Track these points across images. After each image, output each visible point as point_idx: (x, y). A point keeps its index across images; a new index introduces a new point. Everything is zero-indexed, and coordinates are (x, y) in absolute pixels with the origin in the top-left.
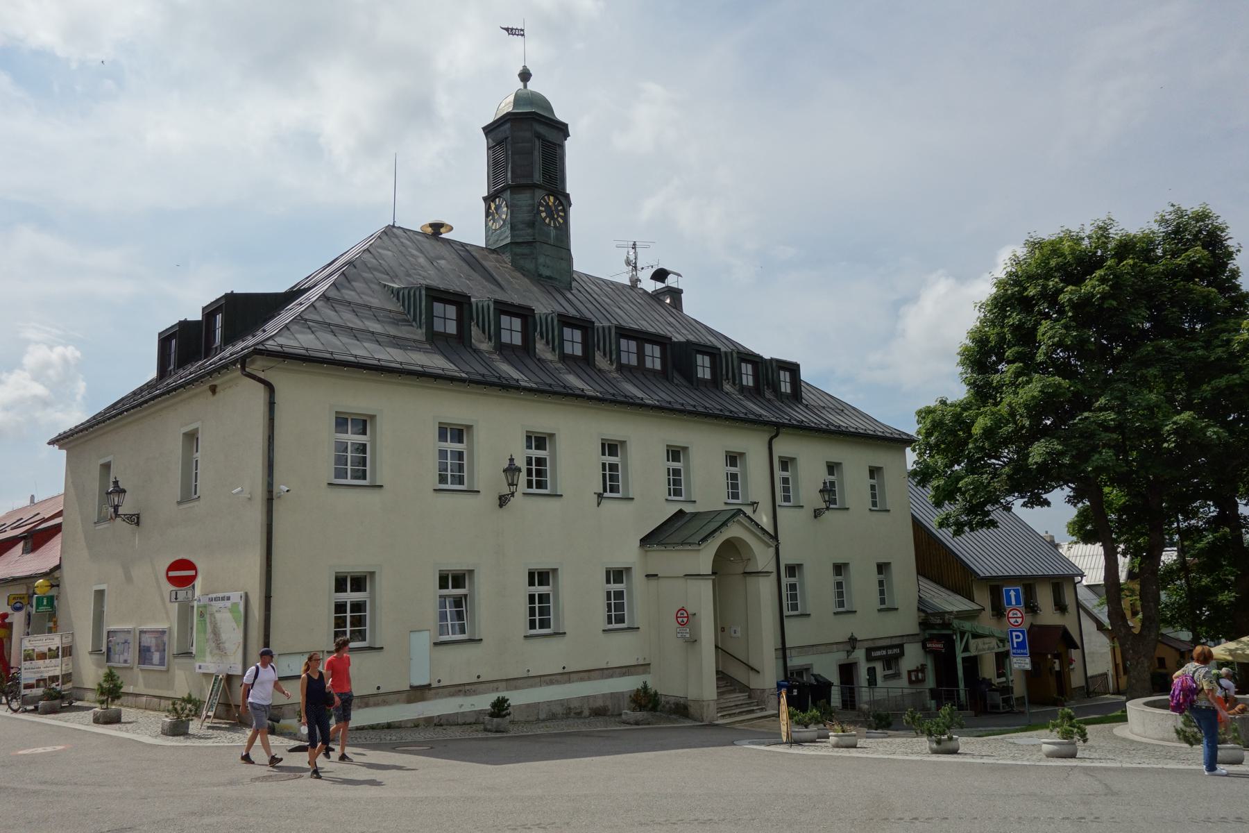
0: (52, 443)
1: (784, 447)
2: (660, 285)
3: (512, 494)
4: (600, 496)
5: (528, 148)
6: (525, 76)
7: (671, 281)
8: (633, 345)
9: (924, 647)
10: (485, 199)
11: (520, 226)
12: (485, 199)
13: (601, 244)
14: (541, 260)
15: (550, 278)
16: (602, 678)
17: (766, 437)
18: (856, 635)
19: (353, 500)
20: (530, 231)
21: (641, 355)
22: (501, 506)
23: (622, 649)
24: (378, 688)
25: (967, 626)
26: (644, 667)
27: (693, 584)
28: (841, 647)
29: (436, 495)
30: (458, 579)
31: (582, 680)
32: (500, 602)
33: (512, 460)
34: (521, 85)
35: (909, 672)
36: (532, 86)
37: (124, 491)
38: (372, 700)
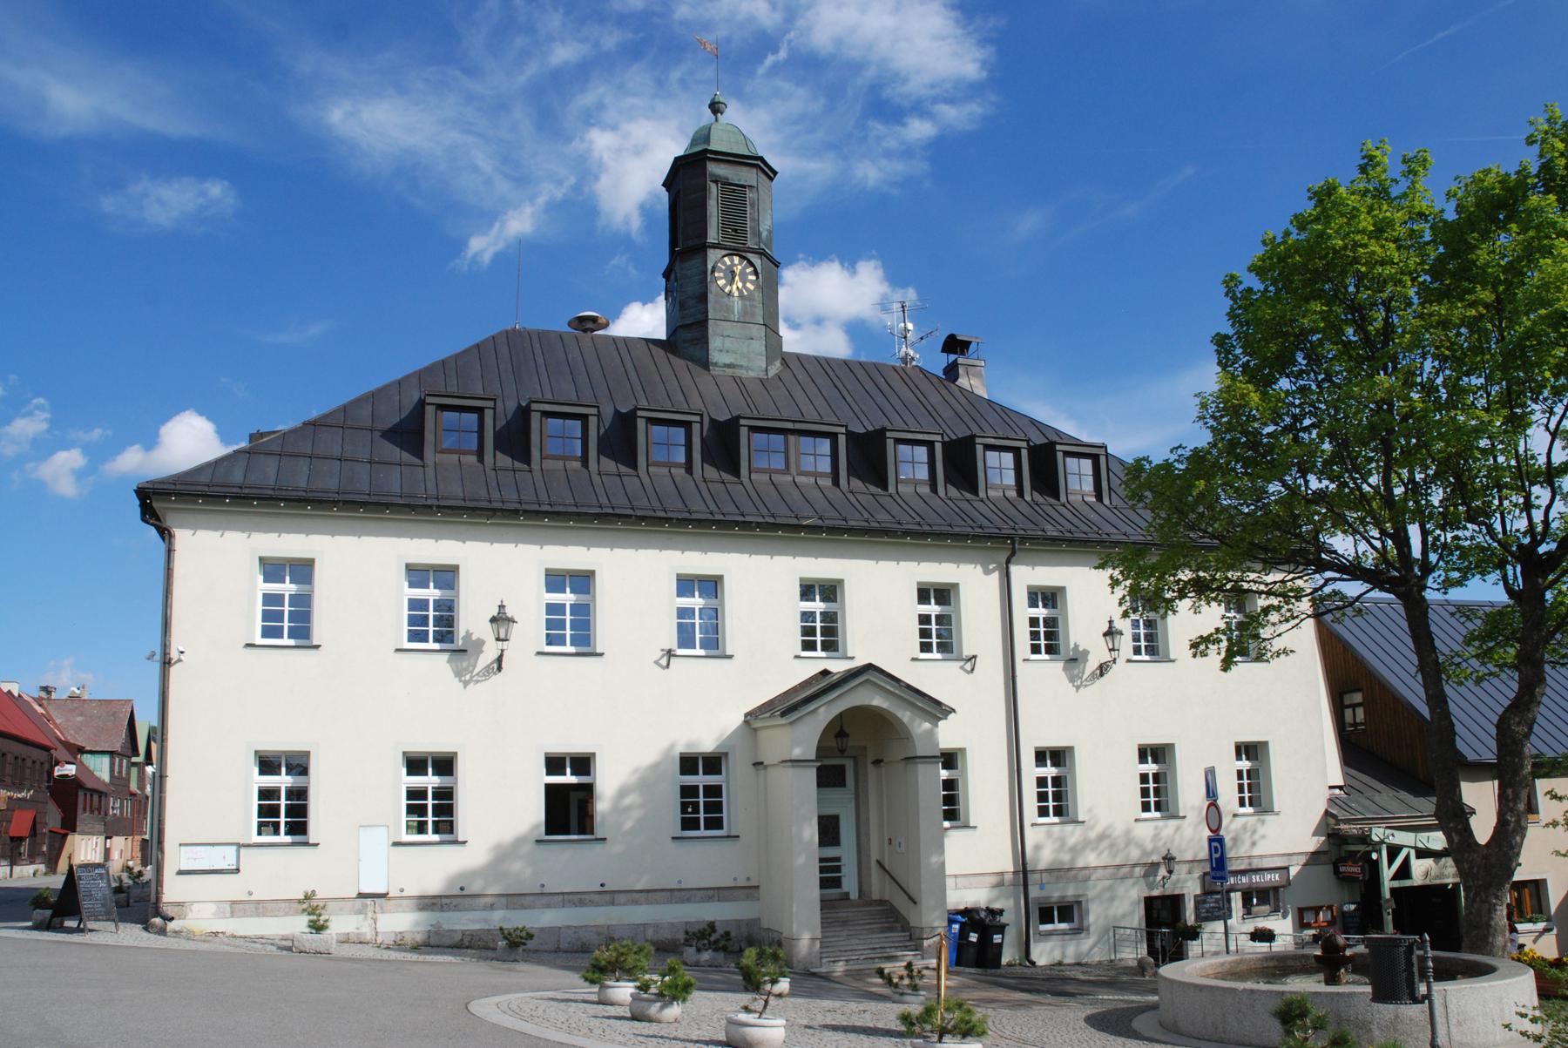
9: (1336, 872)
11: (691, 303)
17: (1003, 557)
18: (1174, 853)
19: (290, 662)
23: (705, 861)
26: (750, 891)
27: (790, 772)
33: (502, 607)
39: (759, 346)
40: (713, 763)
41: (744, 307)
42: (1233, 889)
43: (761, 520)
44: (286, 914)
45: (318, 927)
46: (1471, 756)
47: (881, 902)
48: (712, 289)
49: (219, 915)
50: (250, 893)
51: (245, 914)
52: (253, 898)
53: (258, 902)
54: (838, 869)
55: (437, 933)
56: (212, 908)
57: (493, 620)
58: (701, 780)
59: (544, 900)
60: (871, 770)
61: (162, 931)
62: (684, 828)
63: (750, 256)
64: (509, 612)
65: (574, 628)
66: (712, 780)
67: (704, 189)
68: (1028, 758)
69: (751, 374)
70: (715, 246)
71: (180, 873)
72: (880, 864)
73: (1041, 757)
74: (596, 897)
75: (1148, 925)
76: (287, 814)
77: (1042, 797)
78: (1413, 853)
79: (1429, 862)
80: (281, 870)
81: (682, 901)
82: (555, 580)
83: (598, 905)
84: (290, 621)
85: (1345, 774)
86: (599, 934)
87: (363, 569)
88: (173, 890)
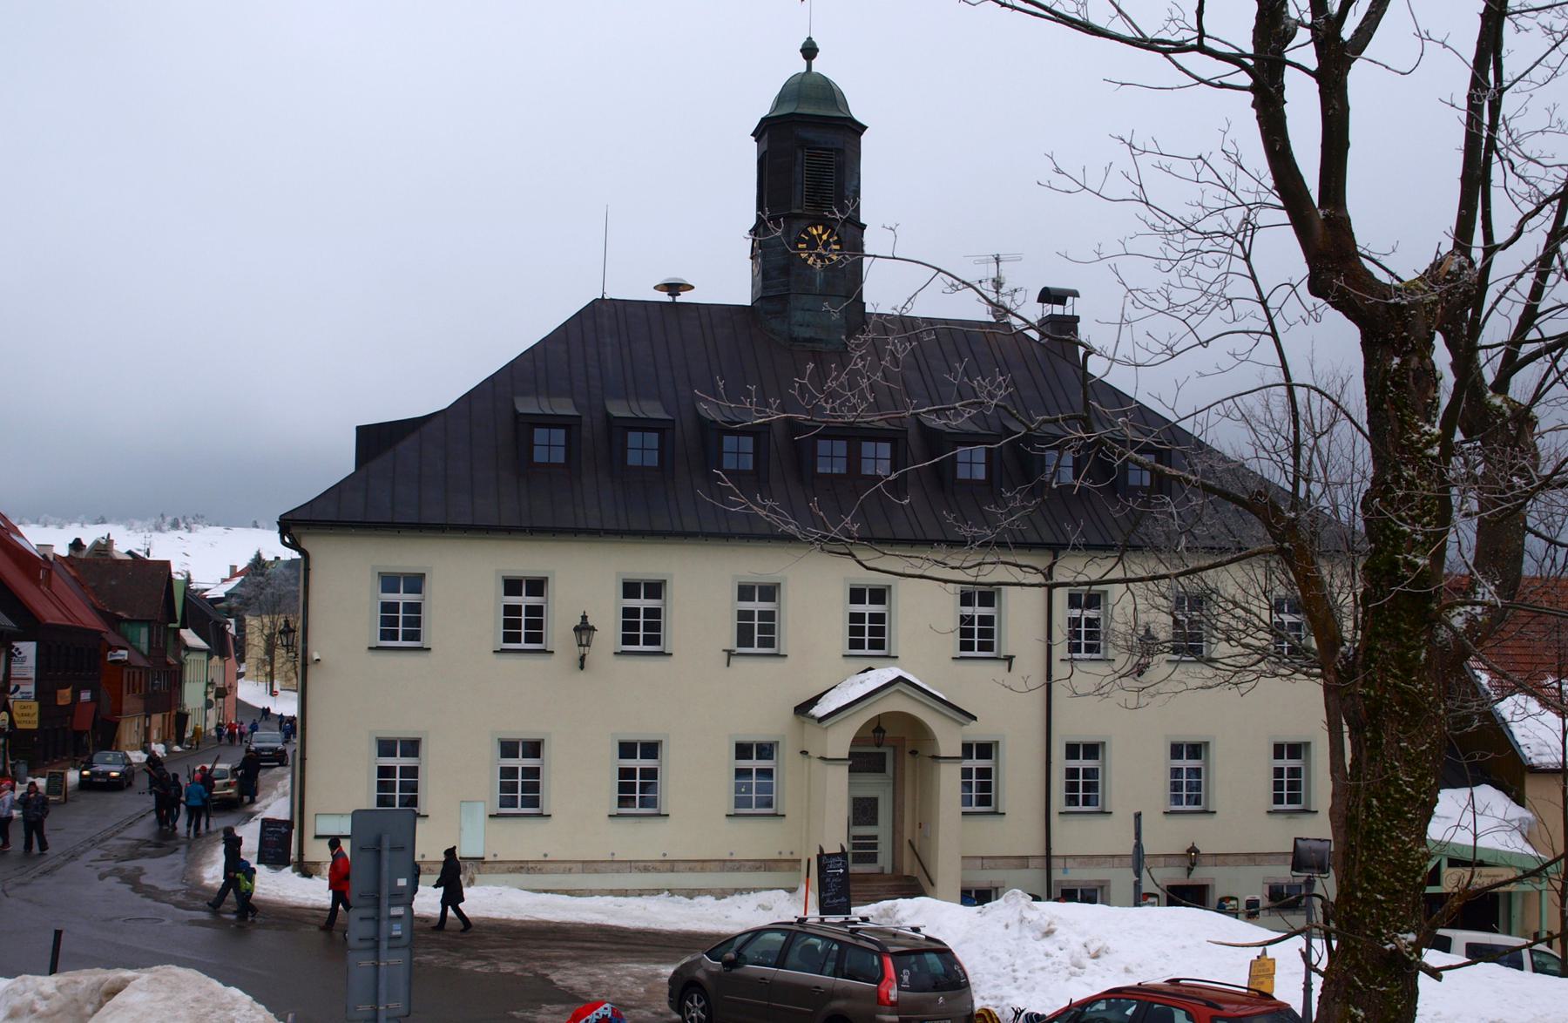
4: (730, 654)
5: (808, 154)
6: (809, 51)
8: (841, 447)
14: (798, 316)
15: (811, 340)
16: (722, 870)
21: (854, 459)
31: (691, 870)
33: (584, 618)
34: (801, 66)
36: (818, 66)
40: (766, 750)
54: (875, 846)
57: (576, 629)
59: (615, 866)
60: (908, 758)
62: (736, 807)
64: (591, 622)
65: (643, 629)
68: (1059, 752)
71: (317, 837)
73: (1072, 751)
77: (1072, 787)
78: (1444, 863)
79: (1459, 871)
81: (733, 870)
83: (659, 871)
84: (401, 625)
87: (464, 581)
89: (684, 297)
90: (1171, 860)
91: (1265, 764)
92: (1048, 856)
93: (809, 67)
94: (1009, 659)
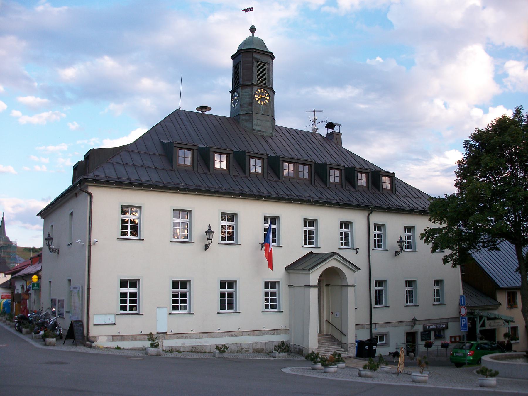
0: (37, 215)
1: (377, 218)
2: (330, 131)
3: (210, 244)
6: (253, 30)
7: (336, 129)
8: (291, 167)
10: (230, 92)
11: (245, 105)
12: (230, 92)
13: (293, 110)
14: (255, 122)
15: (260, 131)
20: (249, 108)
22: (206, 249)
24: (141, 332)
25: (483, 313)
28: (408, 323)
29: (171, 244)
30: (231, 284)
31: (249, 335)
32: (205, 297)
33: (209, 227)
34: (250, 34)
35: (451, 337)
36: (256, 35)
37: (52, 239)
38: (138, 337)
39: (269, 124)
40: (274, 284)
41: (265, 109)
42: (432, 329)
43: (294, 198)
44: (132, 340)
45: (154, 346)
46: (501, 286)
47: (327, 335)
48: (254, 101)
49: (108, 340)
50: (119, 333)
51: (117, 340)
52: (121, 334)
53: (122, 336)
55: (184, 347)
56: (106, 338)
58: (270, 291)
59: (220, 334)
61: (90, 347)
63: (267, 89)
64: (212, 229)
66: (273, 291)
67: (252, 63)
69: (267, 134)
70: (255, 85)
72: (328, 321)
74: (236, 333)
75: (407, 342)
76: (129, 302)
78: (486, 319)
80: (130, 324)
82: (224, 216)
84: (129, 229)
85: (464, 292)
86: (238, 347)
88: (94, 331)
89: (207, 112)
90: (406, 323)
91: (404, 288)
92: (371, 324)
93: (253, 35)
94: (357, 249)
